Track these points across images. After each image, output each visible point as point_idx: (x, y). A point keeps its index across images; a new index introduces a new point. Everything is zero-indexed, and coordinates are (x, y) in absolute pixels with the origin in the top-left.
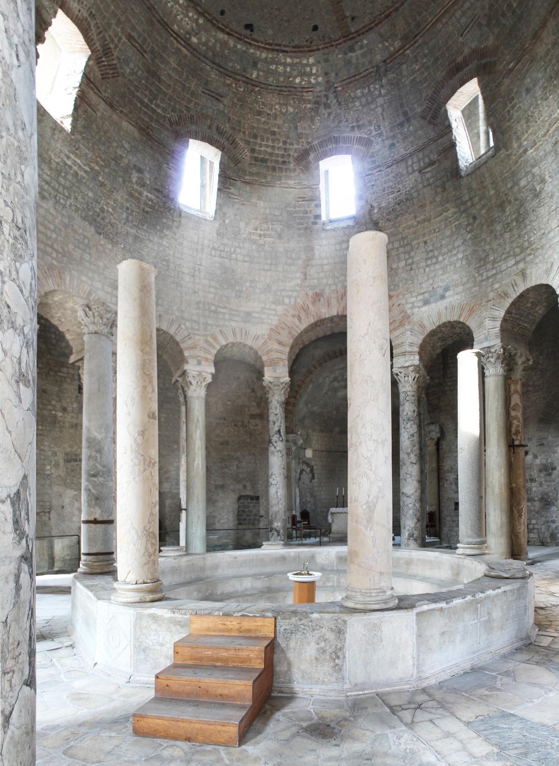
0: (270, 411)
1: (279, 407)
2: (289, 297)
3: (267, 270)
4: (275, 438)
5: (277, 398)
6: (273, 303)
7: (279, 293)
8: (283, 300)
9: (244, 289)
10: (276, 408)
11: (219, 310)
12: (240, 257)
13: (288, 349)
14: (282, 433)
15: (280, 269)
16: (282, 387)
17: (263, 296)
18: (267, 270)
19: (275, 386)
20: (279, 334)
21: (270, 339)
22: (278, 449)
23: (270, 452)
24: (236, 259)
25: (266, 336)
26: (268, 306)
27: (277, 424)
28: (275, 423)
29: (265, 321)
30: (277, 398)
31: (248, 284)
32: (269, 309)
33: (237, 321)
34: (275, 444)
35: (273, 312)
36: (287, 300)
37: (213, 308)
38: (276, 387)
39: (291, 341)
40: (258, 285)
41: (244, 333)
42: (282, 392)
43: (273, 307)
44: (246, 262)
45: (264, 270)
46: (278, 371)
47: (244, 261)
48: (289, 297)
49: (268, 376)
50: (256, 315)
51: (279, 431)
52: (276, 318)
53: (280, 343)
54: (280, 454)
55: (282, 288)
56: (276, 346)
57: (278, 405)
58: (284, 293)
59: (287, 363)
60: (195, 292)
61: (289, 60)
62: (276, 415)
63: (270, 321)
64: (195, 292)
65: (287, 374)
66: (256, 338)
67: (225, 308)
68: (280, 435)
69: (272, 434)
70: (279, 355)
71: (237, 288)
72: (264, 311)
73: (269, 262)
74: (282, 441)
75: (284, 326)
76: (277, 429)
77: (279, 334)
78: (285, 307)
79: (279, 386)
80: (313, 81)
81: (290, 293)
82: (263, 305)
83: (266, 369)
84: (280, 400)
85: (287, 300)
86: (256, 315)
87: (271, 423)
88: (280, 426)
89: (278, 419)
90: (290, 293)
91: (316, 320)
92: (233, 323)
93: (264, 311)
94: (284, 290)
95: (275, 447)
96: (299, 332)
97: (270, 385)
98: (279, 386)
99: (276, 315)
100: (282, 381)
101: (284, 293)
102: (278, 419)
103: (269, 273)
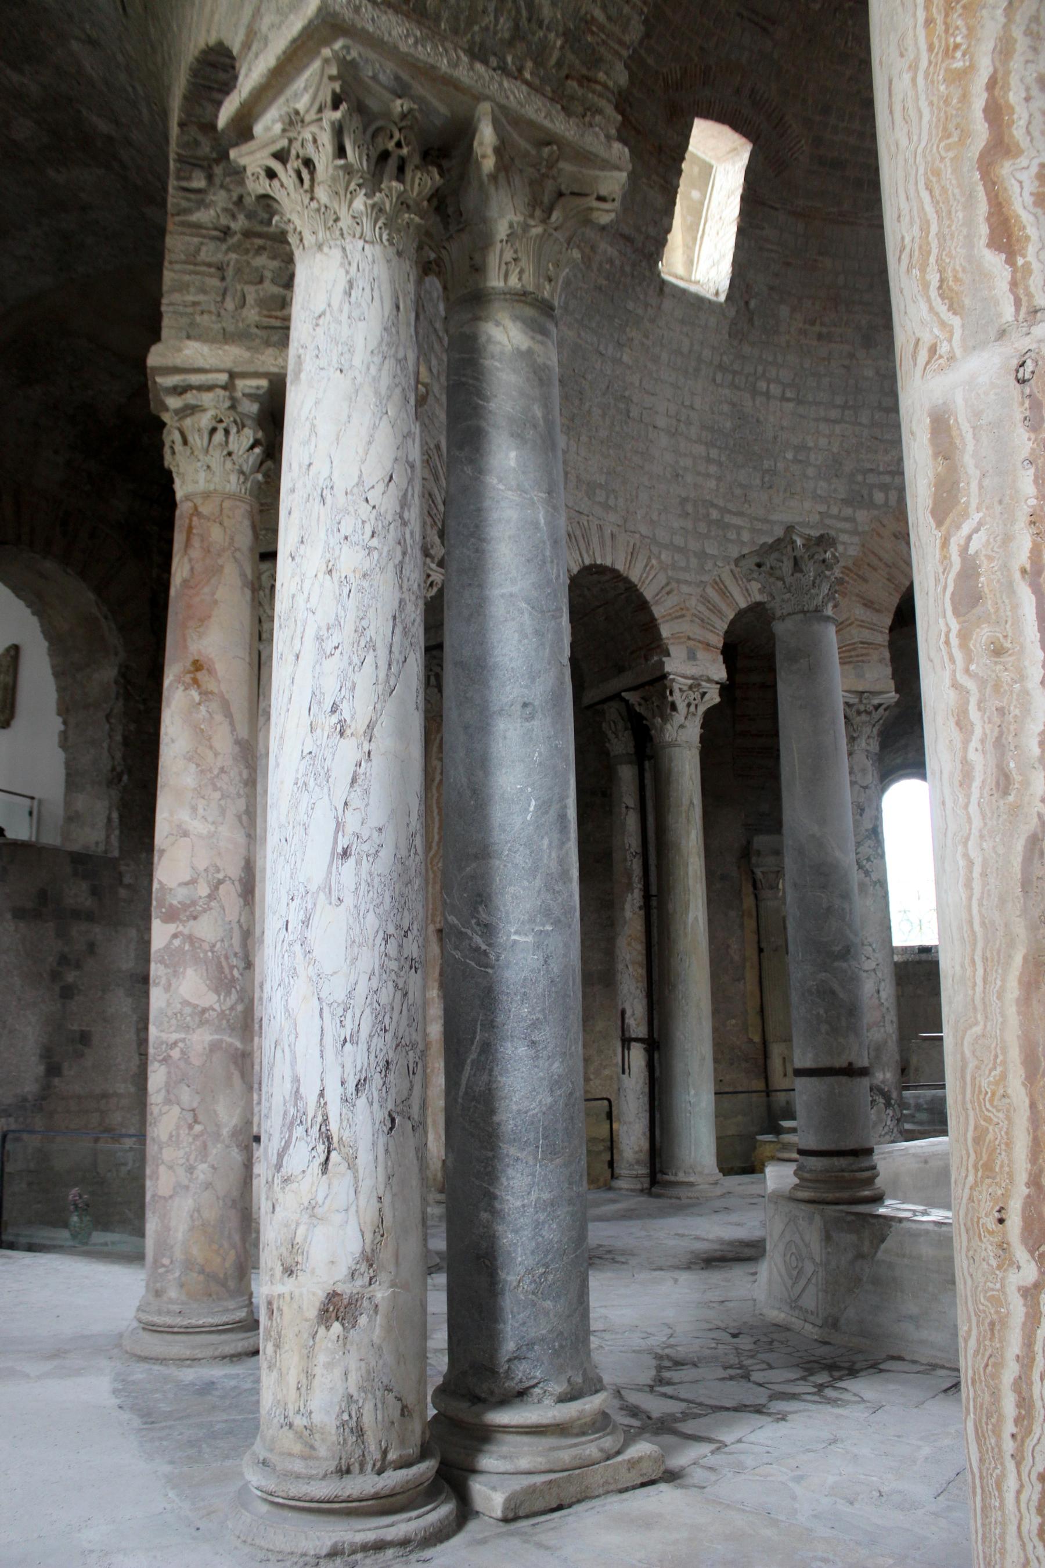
5: (864, 745)
7: (860, 478)
8: (871, 495)
9: (780, 465)
11: (727, 518)
12: (775, 390)
15: (864, 420)
16: (876, 716)
17: (822, 484)
18: (835, 422)
19: (859, 713)
20: (866, 581)
24: (767, 395)
26: (835, 511)
28: (863, 810)
31: (790, 455)
32: (837, 517)
35: (847, 526)
36: (879, 497)
37: (715, 514)
38: (864, 717)
40: (812, 456)
42: (875, 731)
43: (848, 511)
44: (788, 400)
45: (827, 420)
47: (784, 399)
52: (856, 539)
53: (868, 604)
55: (868, 466)
56: (860, 612)
57: (869, 763)
58: (872, 479)
60: (677, 475)
64: (677, 475)
65: (892, 684)
67: (740, 514)
70: (867, 635)
73: (839, 400)
75: (875, 561)
76: (870, 826)
77: (866, 581)
78: (876, 512)
82: (823, 508)
94: (872, 470)
98: (869, 713)
99: (855, 532)
100: (876, 702)
101: (872, 479)
103: (838, 429)
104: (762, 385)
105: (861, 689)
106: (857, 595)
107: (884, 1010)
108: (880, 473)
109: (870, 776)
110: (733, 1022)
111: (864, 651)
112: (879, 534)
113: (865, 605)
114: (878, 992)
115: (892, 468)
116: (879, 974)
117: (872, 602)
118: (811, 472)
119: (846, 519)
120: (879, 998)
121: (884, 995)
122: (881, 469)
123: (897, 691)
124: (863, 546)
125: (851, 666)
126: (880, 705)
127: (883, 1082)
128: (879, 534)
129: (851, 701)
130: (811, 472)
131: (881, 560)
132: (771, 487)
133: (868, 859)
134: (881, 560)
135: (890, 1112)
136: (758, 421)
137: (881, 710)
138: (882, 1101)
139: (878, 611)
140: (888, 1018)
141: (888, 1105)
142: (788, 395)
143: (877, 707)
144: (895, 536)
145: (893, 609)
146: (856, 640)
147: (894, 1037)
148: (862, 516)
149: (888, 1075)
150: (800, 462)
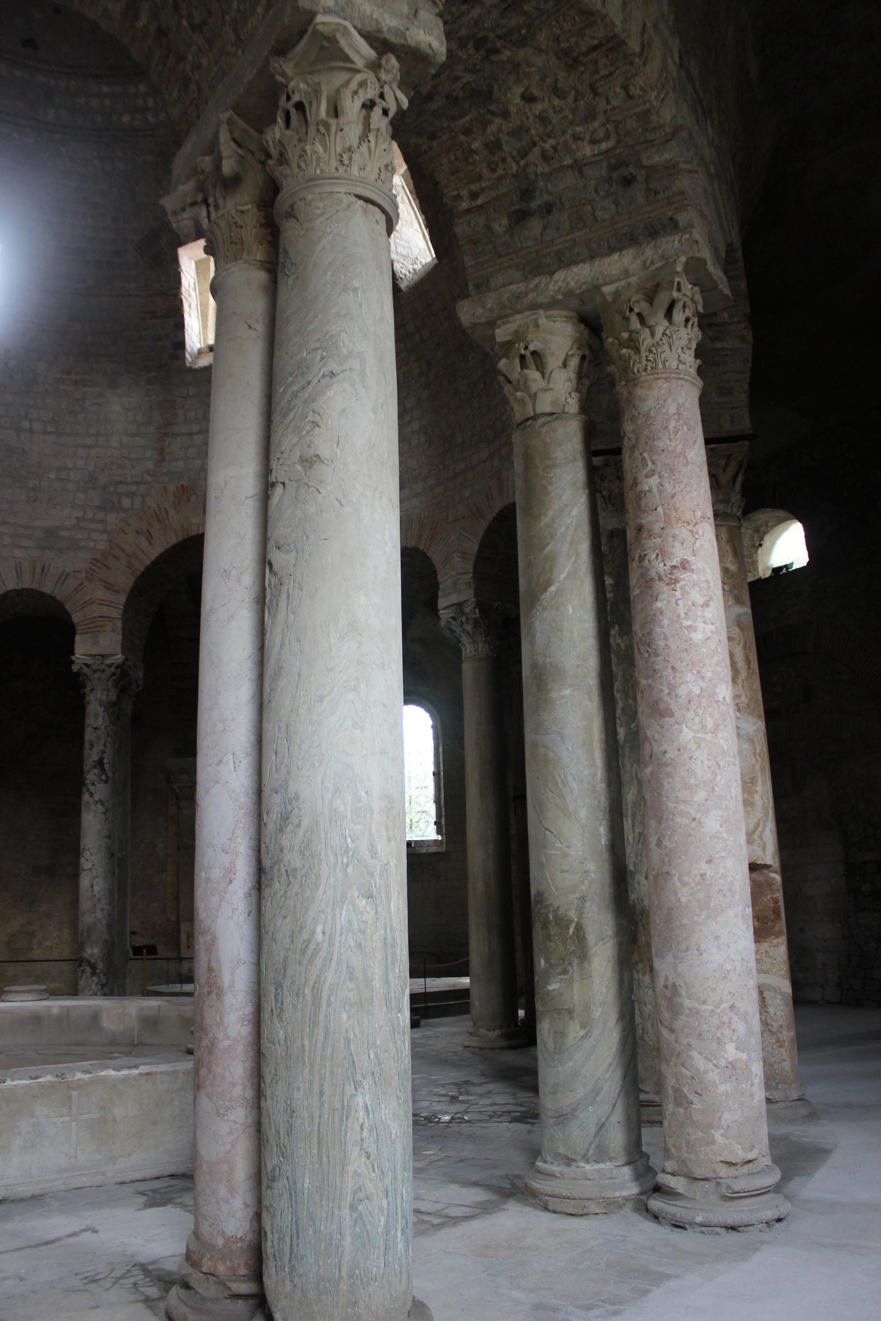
0: (88, 721)
1: (101, 714)
2: (131, 495)
3: (90, 447)
4: (91, 776)
5: (99, 696)
6: (100, 508)
7: (112, 489)
8: (119, 501)
9: (44, 484)
10: (96, 716)
12: (36, 426)
13: (123, 599)
14: (106, 766)
16: (108, 672)
17: (80, 495)
18: (90, 447)
19: (95, 671)
20: (109, 568)
21: (90, 580)
22: (96, 798)
23: (83, 802)
25: (83, 575)
26: (90, 515)
27: (98, 748)
28: (92, 746)
29: (82, 544)
30: (99, 696)
32: (92, 521)
33: (26, 548)
34: (92, 789)
35: (99, 527)
36: (126, 502)
38: (97, 675)
39: (131, 582)
41: (38, 570)
42: (110, 684)
43: (100, 515)
45: (83, 446)
46: (101, 642)
48: (131, 495)
49: (83, 649)
50: (66, 534)
51: (100, 763)
52: (105, 537)
53: (109, 586)
54: (100, 808)
55: (118, 479)
56: (101, 593)
57: (101, 710)
59: (119, 625)
61: (105, 89)
62: (96, 729)
63: (92, 544)
65: (119, 648)
66: (63, 578)
68: (103, 770)
69: (86, 768)
70: (105, 611)
71: (31, 484)
72: (82, 524)
74: (106, 782)
76: (96, 758)
77: (109, 568)
78: (124, 515)
79: (103, 671)
80: (151, 119)
81: (133, 488)
82: (80, 514)
83: (78, 638)
84: (104, 698)
85: (126, 502)
86: (66, 534)
87: (87, 745)
88: (103, 752)
89: (99, 738)
90: (133, 488)
91: (181, 539)
92: (17, 552)
93: (82, 524)
94: (121, 482)
95: (91, 795)
96: (148, 563)
97: (86, 670)
98: (103, 671)
100: (109, 662)
102: (99, 738)
104: (26, 424)
105: (93, 653)
106: (101, 580)
107: (96, 900)
108: (128, 484)
109: (101, 720)
110: (156, 905)
111: (102, 623)
112: (124, 531)
113: (106, 587)
114: (92, 886)
115: (138, 480)
116: (94, 872)
117: (112, 585)
118: (71, 486)
119: (99, 522)
120: (92, 891)
121: (96, 888)
122: (129, 480)
123: (123, 653)
124: (111, 541)
125: (90, 635)
126: (112, 664)
127: (91, 956)
128: (124, 531)
129: (89, 662)
130: (71, 486)
131: (123, 551)
132: (35, 501)
133: (93, 784)
134: (123, 551)
135: (95, 979)
136: (24, 451)
137: (113, 669)
138: (89, 970)
139: (116, 591)
140: (99, 906)
141: (94, 973)
142: (49, 429)
143: (110, 666)
144: (137, 532)
145: (128, 591)
146: (96, 615)
147: (104, 921)
148: (112, 518)
149: (96, 950)
150: (62, 479)
